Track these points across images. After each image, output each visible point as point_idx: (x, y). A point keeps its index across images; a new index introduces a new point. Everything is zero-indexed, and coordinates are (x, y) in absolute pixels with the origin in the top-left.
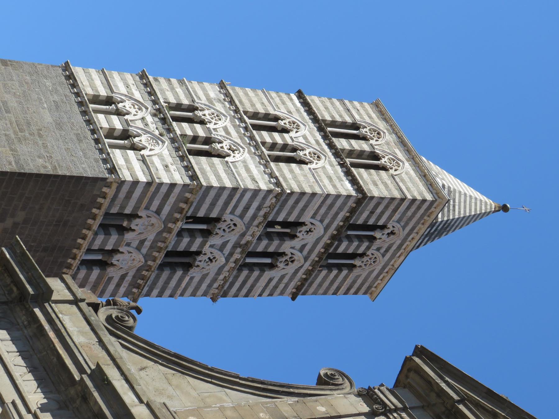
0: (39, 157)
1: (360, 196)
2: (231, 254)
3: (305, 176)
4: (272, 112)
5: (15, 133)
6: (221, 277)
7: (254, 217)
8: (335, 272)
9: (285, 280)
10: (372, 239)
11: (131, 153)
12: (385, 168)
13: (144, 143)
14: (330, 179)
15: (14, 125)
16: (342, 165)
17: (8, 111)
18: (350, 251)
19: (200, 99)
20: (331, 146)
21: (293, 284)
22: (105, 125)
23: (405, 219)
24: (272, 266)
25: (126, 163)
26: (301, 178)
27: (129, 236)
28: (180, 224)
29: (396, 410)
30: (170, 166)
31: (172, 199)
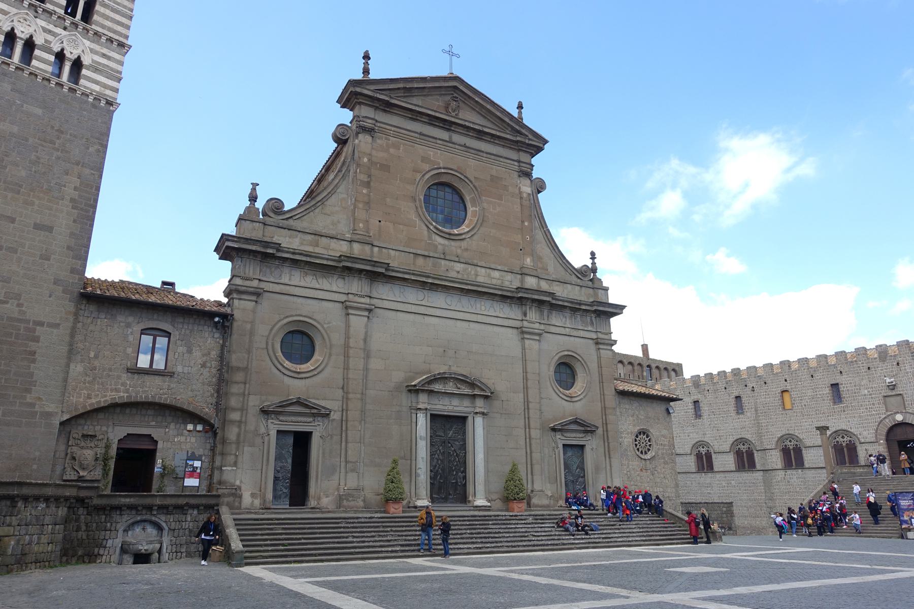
0: (88, 148)
5: (58, 150)
13: (75, 52)
15: (44, 144)
17: (27, 140)
25: (98, 84)
30: (102, 51)
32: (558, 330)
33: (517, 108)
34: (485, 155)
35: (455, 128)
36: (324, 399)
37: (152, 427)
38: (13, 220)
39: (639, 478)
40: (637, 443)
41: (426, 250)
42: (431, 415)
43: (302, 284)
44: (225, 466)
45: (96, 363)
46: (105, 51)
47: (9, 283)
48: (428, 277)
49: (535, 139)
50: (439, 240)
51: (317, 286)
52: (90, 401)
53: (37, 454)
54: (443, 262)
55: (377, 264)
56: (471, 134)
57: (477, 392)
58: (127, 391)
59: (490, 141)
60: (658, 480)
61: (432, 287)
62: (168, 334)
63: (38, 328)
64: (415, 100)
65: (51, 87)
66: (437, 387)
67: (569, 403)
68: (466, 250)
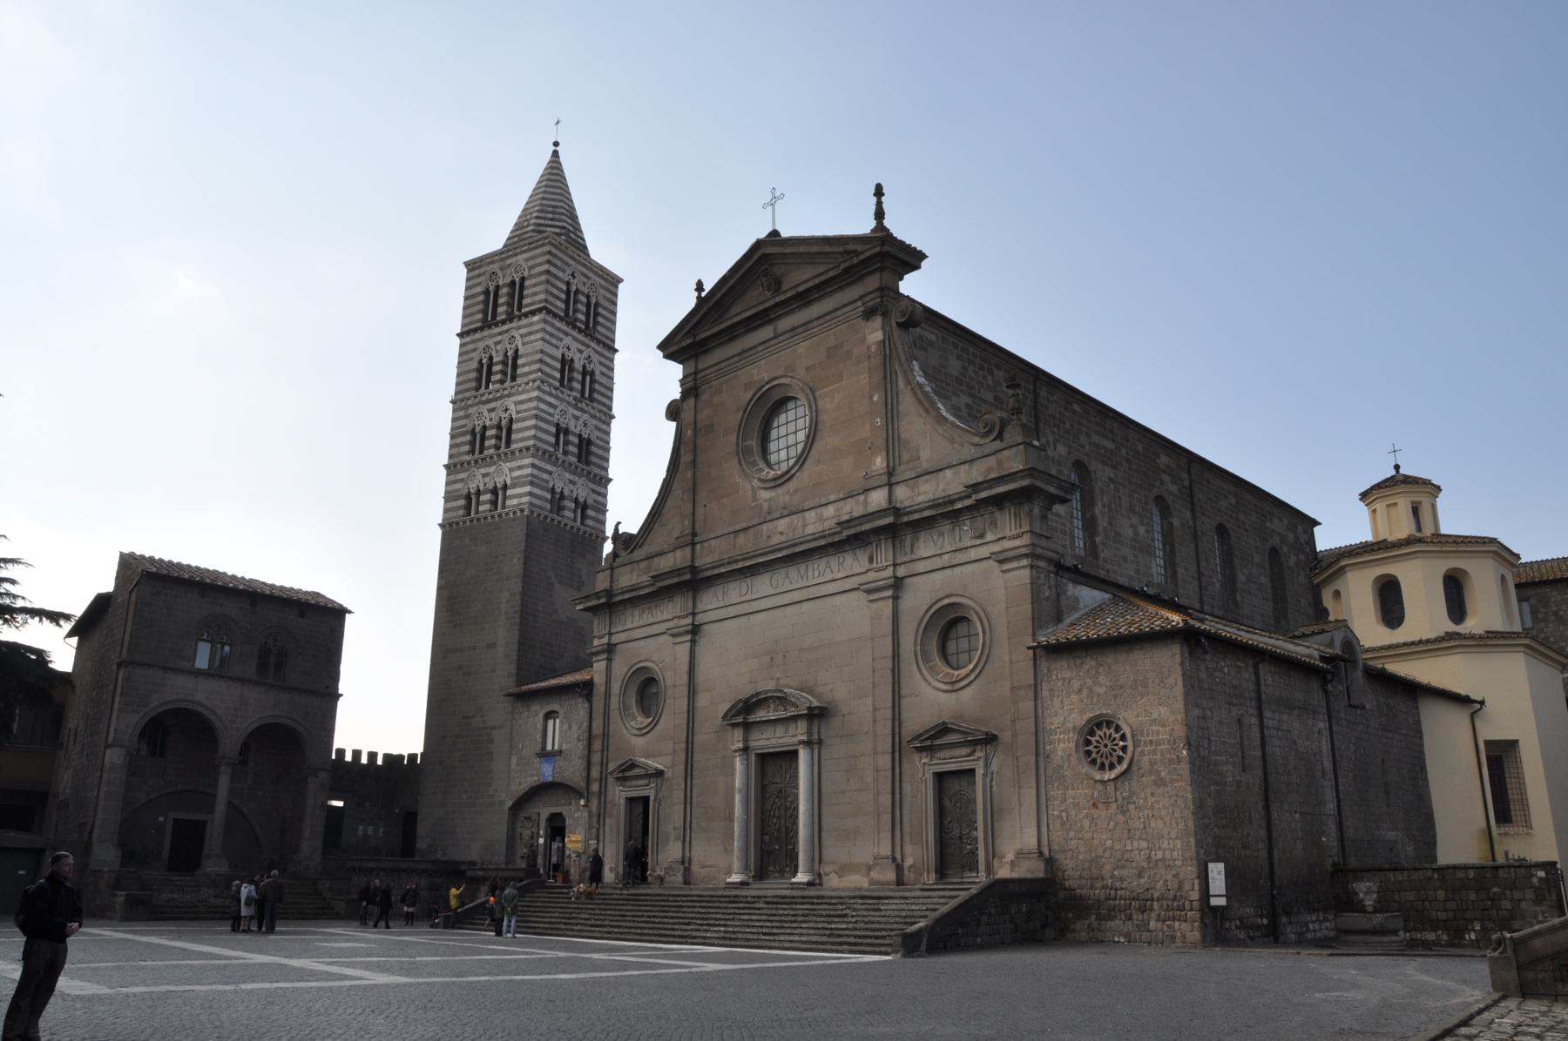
1: (544, 312)
2: (582, 410)
3: (528, 355)
4: (474, 365)
6: (598, 415)
7: (556, 397)
8: (600, 319)
9: (603, 360)
10: (577, 292)
11: (509, 492)
12: (523, 279)
13: (501, 480)
14: (530, 333)
16: (520, 319)
18: (584, 309)
19: (465, 426)
20: (503, 322)
21: (606, 353)
22: (486, 507)
23: (563, 266)
24: (592, 374)
26: (530, 359)
27: (566, 493)
28: (559, 456)
29: (695, 380)
31: (542, 464)
32: (929, 565)
33: (875, 195)
34: (816, 323)
35: (774, 313)
37: (563, 805)
39: (1086, 823)
40: (1091, 748)
42: (757, 755)
43: (641, 623)
46: (520, 463)
48: (737, 561)
49: (867, 247)
50: (765, 495)
51: (652, 620)
54: (765, 527)
55: (681, 572)
56: (794, 306)
57: (792, 712)
59: (821, 296)
60: (1138, 824)
64: (733, 311)
66: (761, 715)
67: (949, 695)
68: (796, 491)
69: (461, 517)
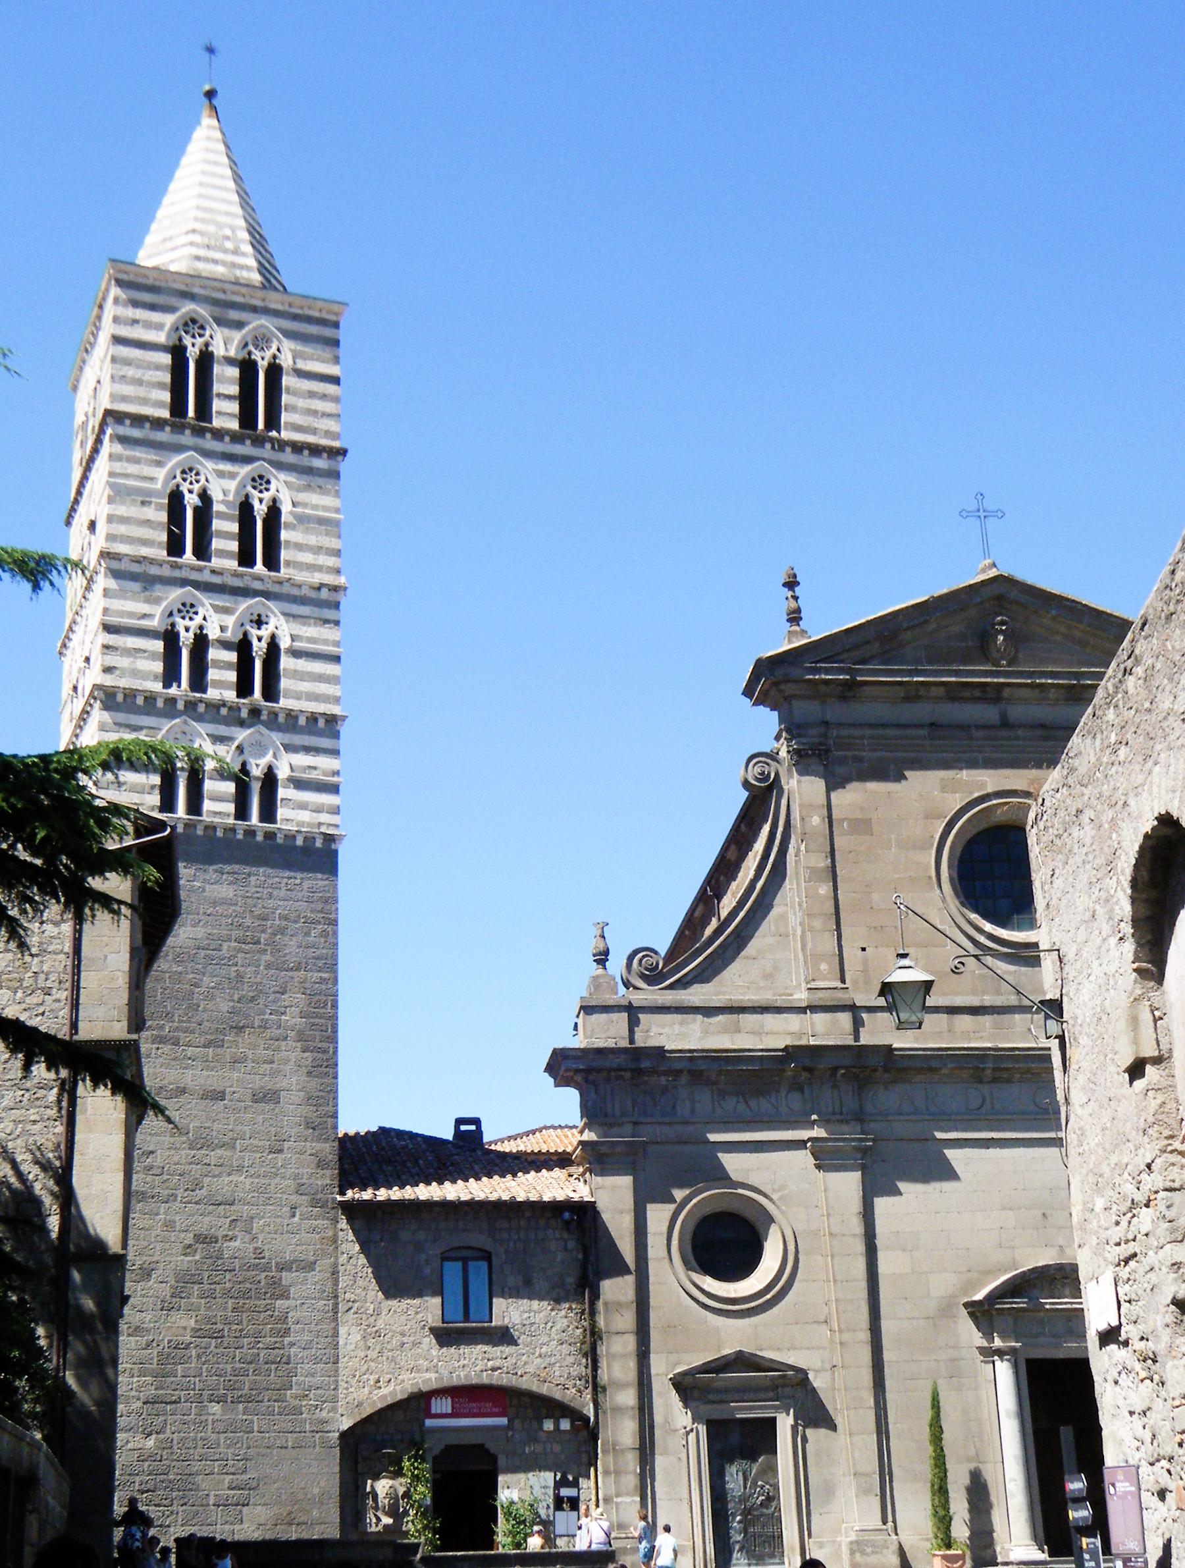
0: (308, 934)
13: (264, 762)
20: (236, 438)
36: (793, 1348)
38: (221, 1096)
41: (974, 992)
44: (617, 1496)
45: (380, 1324)
47: (232, 1204)
52: (378, 1394)
53: (316, 1491)
58: (436, 1369)
61: (998, 1074)
62: (487, 1256)
63: (284, 1274)
65: (239, 841)
69: (152, 808)
